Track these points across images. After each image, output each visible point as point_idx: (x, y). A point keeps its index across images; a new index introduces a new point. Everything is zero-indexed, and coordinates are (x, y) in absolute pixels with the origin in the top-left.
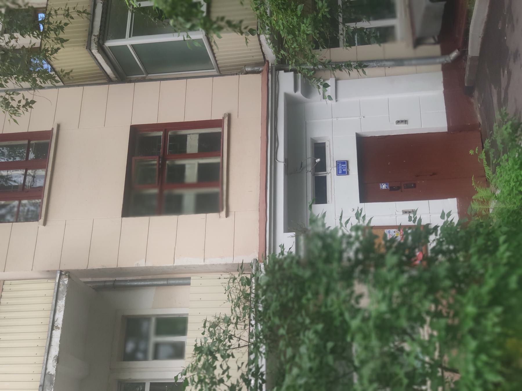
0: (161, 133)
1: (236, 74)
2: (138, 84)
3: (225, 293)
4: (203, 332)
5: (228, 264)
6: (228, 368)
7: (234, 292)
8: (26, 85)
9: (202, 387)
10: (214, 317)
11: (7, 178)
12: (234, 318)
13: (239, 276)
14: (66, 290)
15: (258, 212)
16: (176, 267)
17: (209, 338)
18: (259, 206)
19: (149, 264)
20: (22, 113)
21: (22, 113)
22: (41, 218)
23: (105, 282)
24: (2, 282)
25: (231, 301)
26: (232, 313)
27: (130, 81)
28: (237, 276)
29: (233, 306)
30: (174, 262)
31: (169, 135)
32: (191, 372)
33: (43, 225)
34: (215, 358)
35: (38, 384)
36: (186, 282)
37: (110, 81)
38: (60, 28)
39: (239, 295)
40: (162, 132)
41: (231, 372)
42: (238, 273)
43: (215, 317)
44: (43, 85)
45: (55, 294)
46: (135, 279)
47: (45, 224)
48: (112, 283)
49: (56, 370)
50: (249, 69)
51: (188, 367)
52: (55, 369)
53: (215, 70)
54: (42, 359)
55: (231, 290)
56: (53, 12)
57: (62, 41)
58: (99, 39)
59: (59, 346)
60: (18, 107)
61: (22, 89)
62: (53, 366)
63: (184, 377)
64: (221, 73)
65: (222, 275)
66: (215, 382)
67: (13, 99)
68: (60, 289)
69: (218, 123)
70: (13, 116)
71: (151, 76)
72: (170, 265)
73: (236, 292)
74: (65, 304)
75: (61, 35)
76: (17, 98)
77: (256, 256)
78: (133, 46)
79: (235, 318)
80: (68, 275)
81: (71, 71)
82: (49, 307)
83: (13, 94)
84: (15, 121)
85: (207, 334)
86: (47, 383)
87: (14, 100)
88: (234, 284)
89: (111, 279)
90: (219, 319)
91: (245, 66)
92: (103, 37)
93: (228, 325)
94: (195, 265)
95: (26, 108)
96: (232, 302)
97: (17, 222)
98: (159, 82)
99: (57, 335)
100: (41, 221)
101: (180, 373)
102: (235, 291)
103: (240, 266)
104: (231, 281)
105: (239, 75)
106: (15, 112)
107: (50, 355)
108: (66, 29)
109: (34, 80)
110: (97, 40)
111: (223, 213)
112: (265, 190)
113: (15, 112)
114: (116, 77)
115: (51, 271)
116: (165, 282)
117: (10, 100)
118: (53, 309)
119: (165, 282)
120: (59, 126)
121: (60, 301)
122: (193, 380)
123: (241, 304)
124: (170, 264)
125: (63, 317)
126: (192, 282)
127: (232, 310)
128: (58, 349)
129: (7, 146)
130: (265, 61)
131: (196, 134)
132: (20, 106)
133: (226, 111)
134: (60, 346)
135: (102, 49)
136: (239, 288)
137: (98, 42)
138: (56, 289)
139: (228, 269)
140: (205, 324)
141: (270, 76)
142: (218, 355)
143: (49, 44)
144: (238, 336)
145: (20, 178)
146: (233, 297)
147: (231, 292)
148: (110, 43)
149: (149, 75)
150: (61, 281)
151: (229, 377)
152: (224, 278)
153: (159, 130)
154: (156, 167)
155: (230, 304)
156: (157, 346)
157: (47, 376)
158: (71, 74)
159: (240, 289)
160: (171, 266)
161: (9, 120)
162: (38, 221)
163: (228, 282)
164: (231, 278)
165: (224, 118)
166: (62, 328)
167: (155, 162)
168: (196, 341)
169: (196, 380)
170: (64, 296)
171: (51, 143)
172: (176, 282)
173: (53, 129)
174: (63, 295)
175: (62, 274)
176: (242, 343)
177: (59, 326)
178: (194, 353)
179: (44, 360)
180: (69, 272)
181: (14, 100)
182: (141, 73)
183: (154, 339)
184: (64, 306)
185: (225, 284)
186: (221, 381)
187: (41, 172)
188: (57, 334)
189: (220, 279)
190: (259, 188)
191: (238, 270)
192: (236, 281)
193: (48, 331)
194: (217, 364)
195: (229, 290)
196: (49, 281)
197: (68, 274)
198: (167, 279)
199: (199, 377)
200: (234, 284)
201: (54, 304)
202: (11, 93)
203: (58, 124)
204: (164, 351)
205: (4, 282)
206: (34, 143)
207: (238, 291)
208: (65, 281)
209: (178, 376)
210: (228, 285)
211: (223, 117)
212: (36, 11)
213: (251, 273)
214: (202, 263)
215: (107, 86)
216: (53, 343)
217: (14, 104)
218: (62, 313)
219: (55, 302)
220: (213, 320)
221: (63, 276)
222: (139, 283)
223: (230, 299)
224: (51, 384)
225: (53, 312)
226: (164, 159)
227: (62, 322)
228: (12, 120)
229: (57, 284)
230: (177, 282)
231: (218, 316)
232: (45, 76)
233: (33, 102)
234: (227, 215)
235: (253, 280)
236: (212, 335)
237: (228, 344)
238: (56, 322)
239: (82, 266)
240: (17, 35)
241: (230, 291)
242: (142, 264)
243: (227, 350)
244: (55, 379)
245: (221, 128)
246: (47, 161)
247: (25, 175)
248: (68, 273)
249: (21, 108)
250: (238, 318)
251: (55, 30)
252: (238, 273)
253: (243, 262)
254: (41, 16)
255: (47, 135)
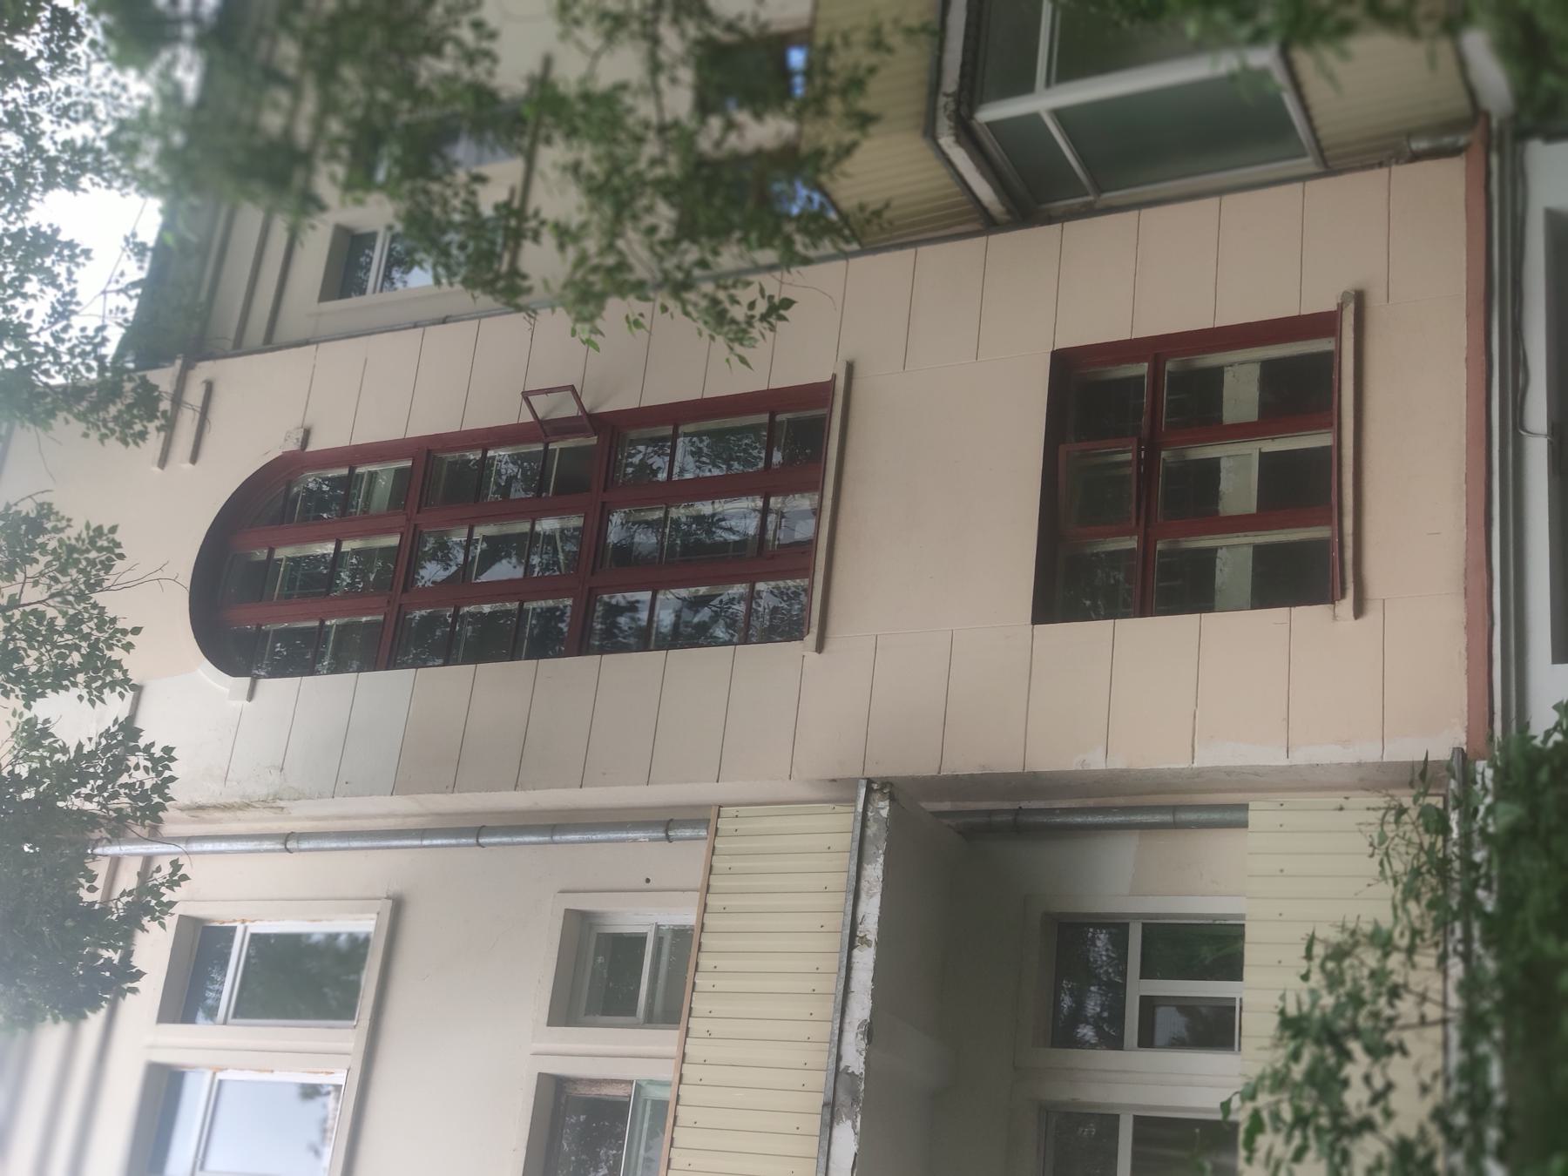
0: (1143, 369)
1: (1381, 165)
2: (1073, 227)
3: (1372, 856)
4: (1303, 971)
5: (1365, 763)
6: (1389, 1086)
7: (1399, 853)
8: (768, 256)
9: (1305, 1138)
10: (1340, 929)
11: (709, 523)
12: (1402, 935)
13: (1415, 802)
14: (885, 835)
15: (1461, 600)
16: (1200, 773)
17: (1324, 992)
18: (1466, 578)
19: (1118, 762)
20: (757, 336)
21: (757, 336)
22: (811, 630)
23: (990, 813)
24: (714, 811)
25: (1391, 882)
26: (1396, 916)
27: (1050, 220)
28: (1407, 801)
29: (1399, 896)
30: (1193, 758)
31: (1169, 372)
32: (1272, 1091)
33: (816, 651)
34: (1346, 1055)
35: (819, 1100)
36: (1233, 818)
37: (989, 224)
38: (856, 84)
39: (1415, 862)
40: (1146, 364)
41: (1395, 1100)
42: (1413, 792)
43: (1343, 928)
44: (812, 253)
45: (856, 845)
46: (1078, 806)
47: (820, 648)
48: (1010, 818)
49: (865, 1063)
50: (1420, 145)
51: (1261, 1078)
52: (862, 1059)
53: (1309, 160)
54: (826, 1030)
55: (1391, 846)
56: (837, 41)
57: (864, 121)
58: (958, 103)
59: (872, 995)
60: (750, 320)
61: (758, 269)
62: (857, 1051)
63: (1250, 1106)
64: (1332, 162)
65: (1347, 798)
66: (1345, 1130)
67: (734, 301)
68: (870, 832)
69: (1324, 324)
70: (736, 346)
71: (1111, 197)
72: (1182, 766)
73: (1407, 853)
74: (883, 875)
75: (863, 104)
76: (745, 296)
77: (1460, 739)
78: (1058, 114)
79: (1407, 934)
80: (890, 792)
81: (887, 206)
82: (841, 881)
83: (734, 286)
84: (743, 360)
85: (1317, 979)
86: (843, 1097)
87: (738, 303)
88: (1398, 827)
89: (1007, 805)
90: (1353, 933)
91: (1411, 134)
92: (972, 93)
93: (1386, 955)
94: (1259, 766)
95: (769, 323)
96: (1396, 884)
97: (745, 643)
98: (1136, 212)
99: (865, 964)
100: (811, 638)
101: (1236, 1093)
102: (1402, 849)
103: (1418, 770)
104: (1391, 818)
105: (1389, 166)
106: (740, 335)
107: (847, 1020)
108: (874, 85)
109: (789, 242)
110: (952, 107)
111: (1346, 606)
112: (1483, 529)
113: (740, 334)
114: (1009, 212)
115: (841, 779)
116: (1168, 818)
117: (727, 305)
118: (852, 888)
119: (1168, 818)
120: (850, 368)
121: (870, 866)
122: (1276, 1116)
123: (1423, 890)
124: (1181, 763)
125: (880, 913)
126: (1253, 817)
127: (1395, 908)
128: (868, 1003)
129: (709, 433)
130: (1477, 114)
131: (1253, 362)
132: (752, 317)
133: (1348, 283)
134: (875, 996)
135: (967, 133)
136: (1416, 839)
137: (957, 111)
138: (858, 832)
139: (1376, 778)
140: (1309, 949)
141: (1495, 161)
142: (1355, 1046)
143: (828, 133)
144: (1420, 989)
145: (743, 521)
146: (1399, 866)
147: (1390, 851)
148: (991, 113)
149: (1106, 195)
150: (871, 808)
151: (1389, 1114)
152: (1368, 809)
153: (1137, 360)
154: (1130, 471)
155: (1387, 890)
156: (1149, 1005)
157: (842, 1077)
158: (887, 215)
159: (1421, 845)
160: (1183, 769)
161: (728, 360)
162: (802, 640)
163: (1380, 822)
164: (1388, 809)
165: (1341, 307)
166: (877, 944)
167: (1129, 456)
168: (1283, 998)
169: (1287, 1114)
170: (881, 852)
171: (830, 417)
172: (1202, 818)
173: (834, 376)
174: (878, 849)
175: (872, 788)
176: (1433, 1012)
177: (868, 937)
178: (1278, 1034)
179: (832, 1033)
180: (892, 785)
181: (738, 303)
182: (1078, 190)
183: (1138, 988)
184: (881, 879)
185: (1372, 828)
186: (1367, 1125)
187: (803, 502)
188: (865, 959)
189: (1341, 809)
190: (1465, 521)
191: (1411, 785)
192: (1405, 818)
193: (841, 951)
194: (1353, 1071)
195: (1384, 846)
196: (838, 808)
197: (886, 787)
198: (1174, 809)
199: (1297, 1111)
200: (1398, 827)
201: (854, 874)
202: (730, 282)
203: (847, 362)
204: (1170, 1022)
205: (719, 810)
206: (784, 421)
207: (1413, 851)
208: (883, 809)
209: (1229, 1101)
210: (1379, 829)
211: (1338, 304)
212: (781, 42)
213: (1442, 791)
214: (1282, 761)
215: (981, 240)
216: (854, 985)
217: (738, 313)
218: (876, 901)
219: (855, 868)
220: (1335, 936)
221: (877, 796)
222: (1091, 819)
223: (1388, 873)
224: (855, 1100)
225: (851, 897)
226: (1152, 447)
227: (876, 926)
228: (734, 360)
229: (860, 818)
230: (1204, 816)
231: (1351, 925)
232: (816, 226)
233: (788, 303)
234: (1359, 610)
235: (1454, 817)
236: (1334, 981)
237: (1388, 1012)
238: (860, 926)
239: (923, 766)
240: (743, 117)
241: (1387, 848)
242: (1096, 761)
243: (1383, 1032)
244: (863, 1087)
245: (1333, 340)
246: (822, 471)
247: (765, 511)
248: (888, 785)
249: (757, 324)
250: (1416, 933)
251: (844, 92)
252: (1413, 792)
253: (1429, 759)
254: (797, 58)
255: (818, 394)
